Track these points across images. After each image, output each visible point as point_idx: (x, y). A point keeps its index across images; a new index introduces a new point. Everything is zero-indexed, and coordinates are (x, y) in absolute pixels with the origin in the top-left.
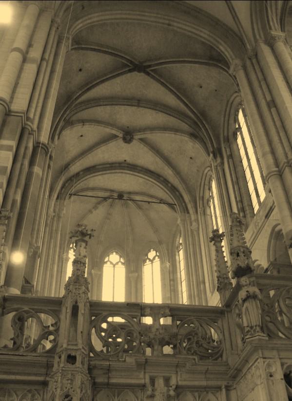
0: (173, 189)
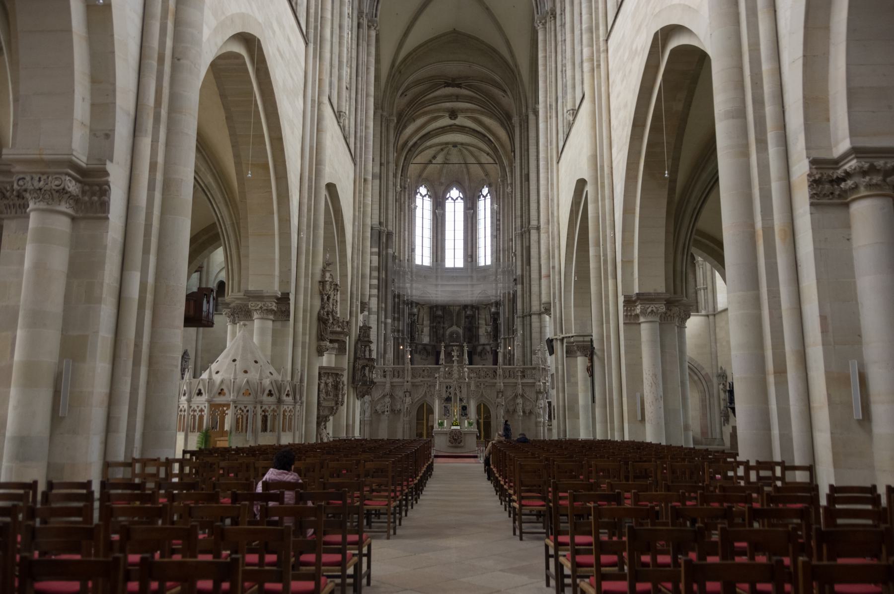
0: (495, 150)
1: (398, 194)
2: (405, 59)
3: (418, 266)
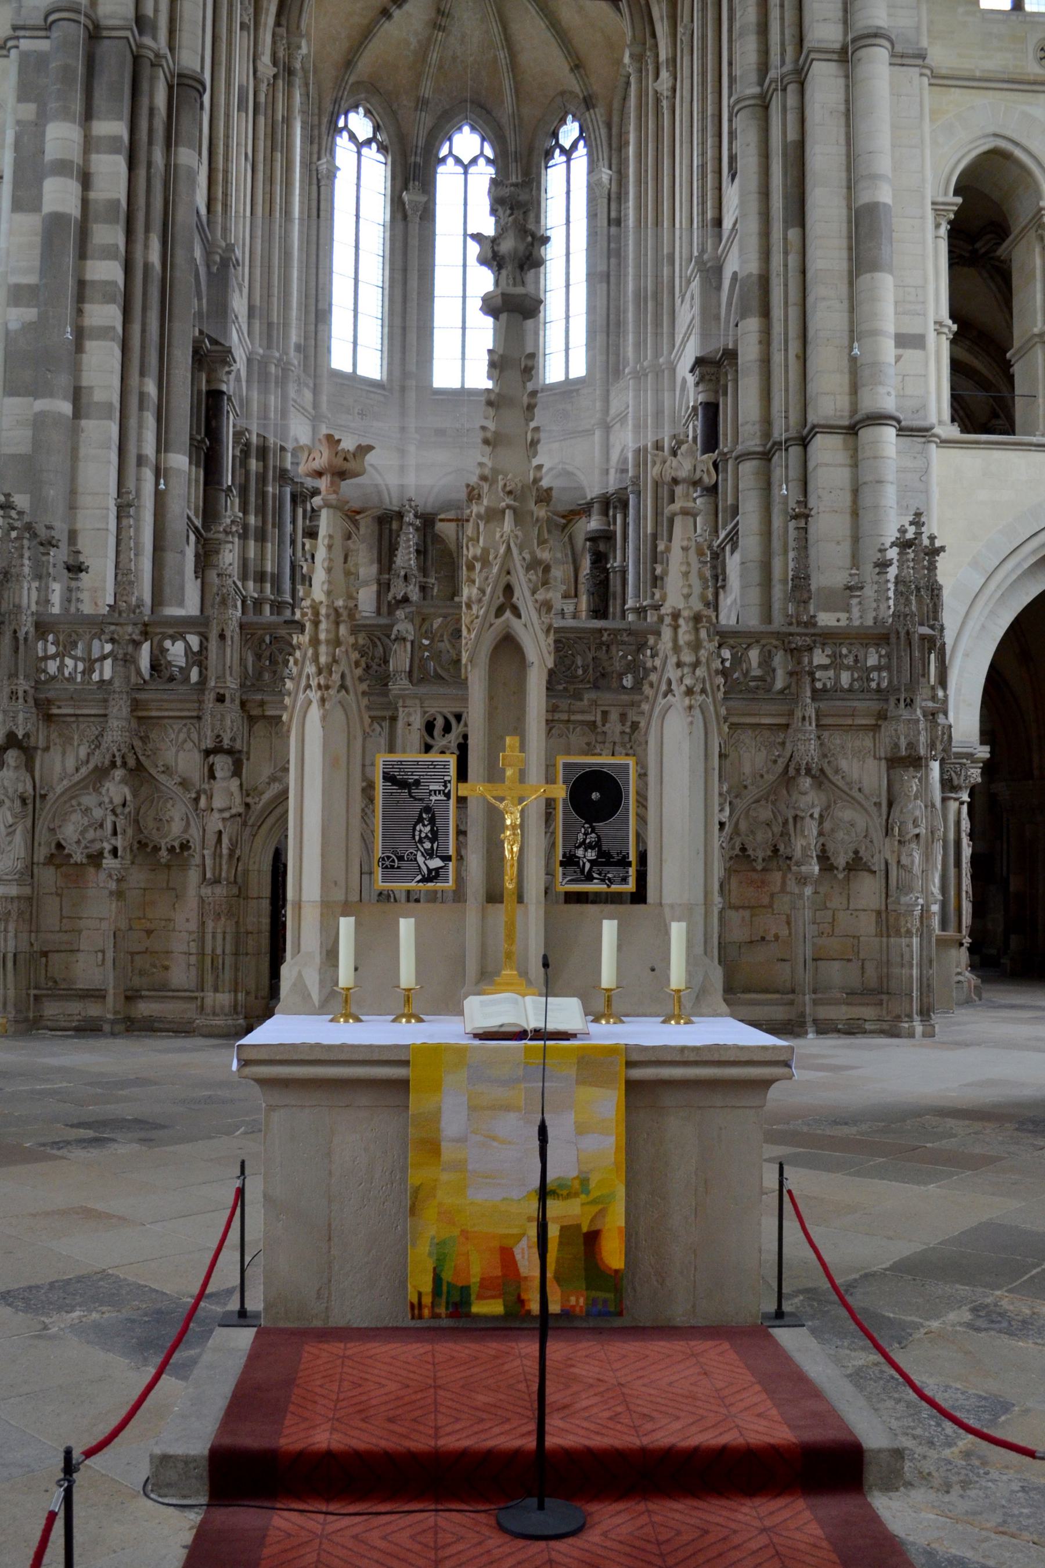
3: (338, 374)
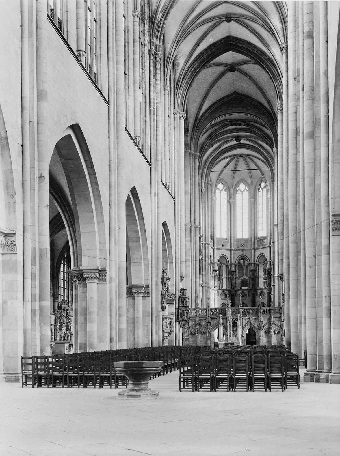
0: (267, 159)
1: (203, 193)
2: (202, 116)
